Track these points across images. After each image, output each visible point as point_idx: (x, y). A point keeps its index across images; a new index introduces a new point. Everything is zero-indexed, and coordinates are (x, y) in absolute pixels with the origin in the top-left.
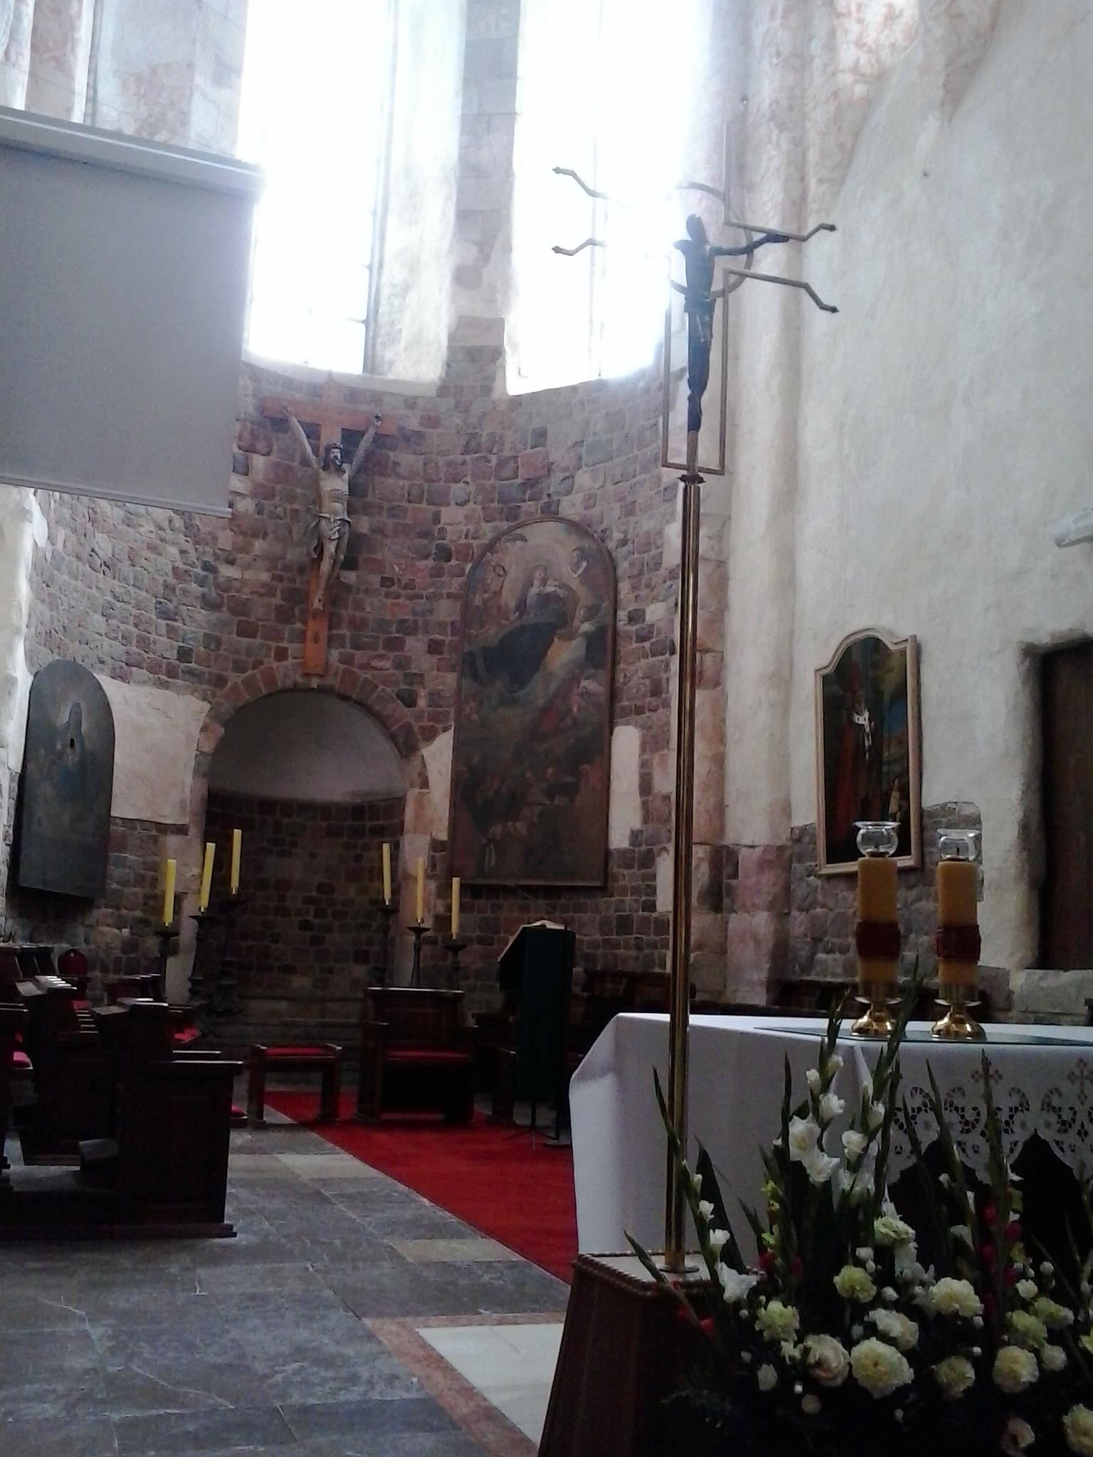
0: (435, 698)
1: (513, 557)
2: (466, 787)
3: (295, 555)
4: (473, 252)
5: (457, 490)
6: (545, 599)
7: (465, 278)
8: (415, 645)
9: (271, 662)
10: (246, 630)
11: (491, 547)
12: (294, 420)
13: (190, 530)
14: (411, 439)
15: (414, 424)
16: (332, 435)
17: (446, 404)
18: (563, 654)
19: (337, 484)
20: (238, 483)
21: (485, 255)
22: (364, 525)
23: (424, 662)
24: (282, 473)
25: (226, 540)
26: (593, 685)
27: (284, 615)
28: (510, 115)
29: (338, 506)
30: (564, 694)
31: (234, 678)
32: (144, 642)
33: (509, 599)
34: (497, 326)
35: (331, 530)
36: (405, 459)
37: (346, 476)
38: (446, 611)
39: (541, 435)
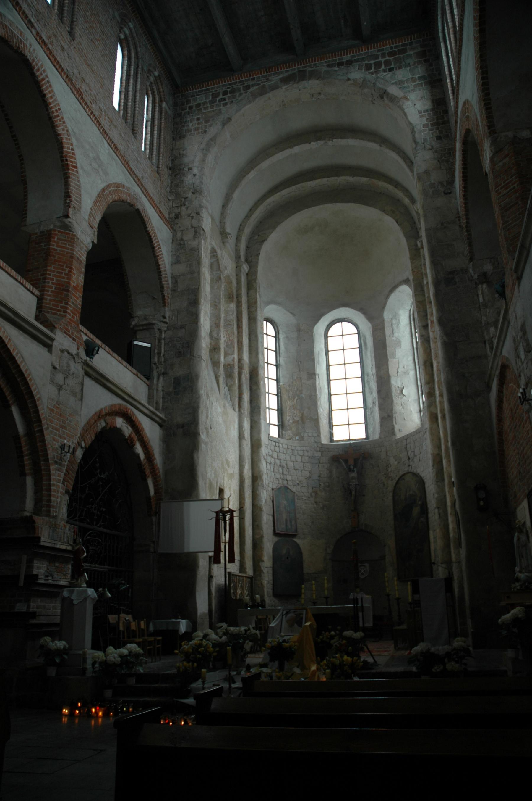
12: (341, 460)
16: (351, 462)
18: (416, 511)
29: (354, 481)
37: (356, 472)
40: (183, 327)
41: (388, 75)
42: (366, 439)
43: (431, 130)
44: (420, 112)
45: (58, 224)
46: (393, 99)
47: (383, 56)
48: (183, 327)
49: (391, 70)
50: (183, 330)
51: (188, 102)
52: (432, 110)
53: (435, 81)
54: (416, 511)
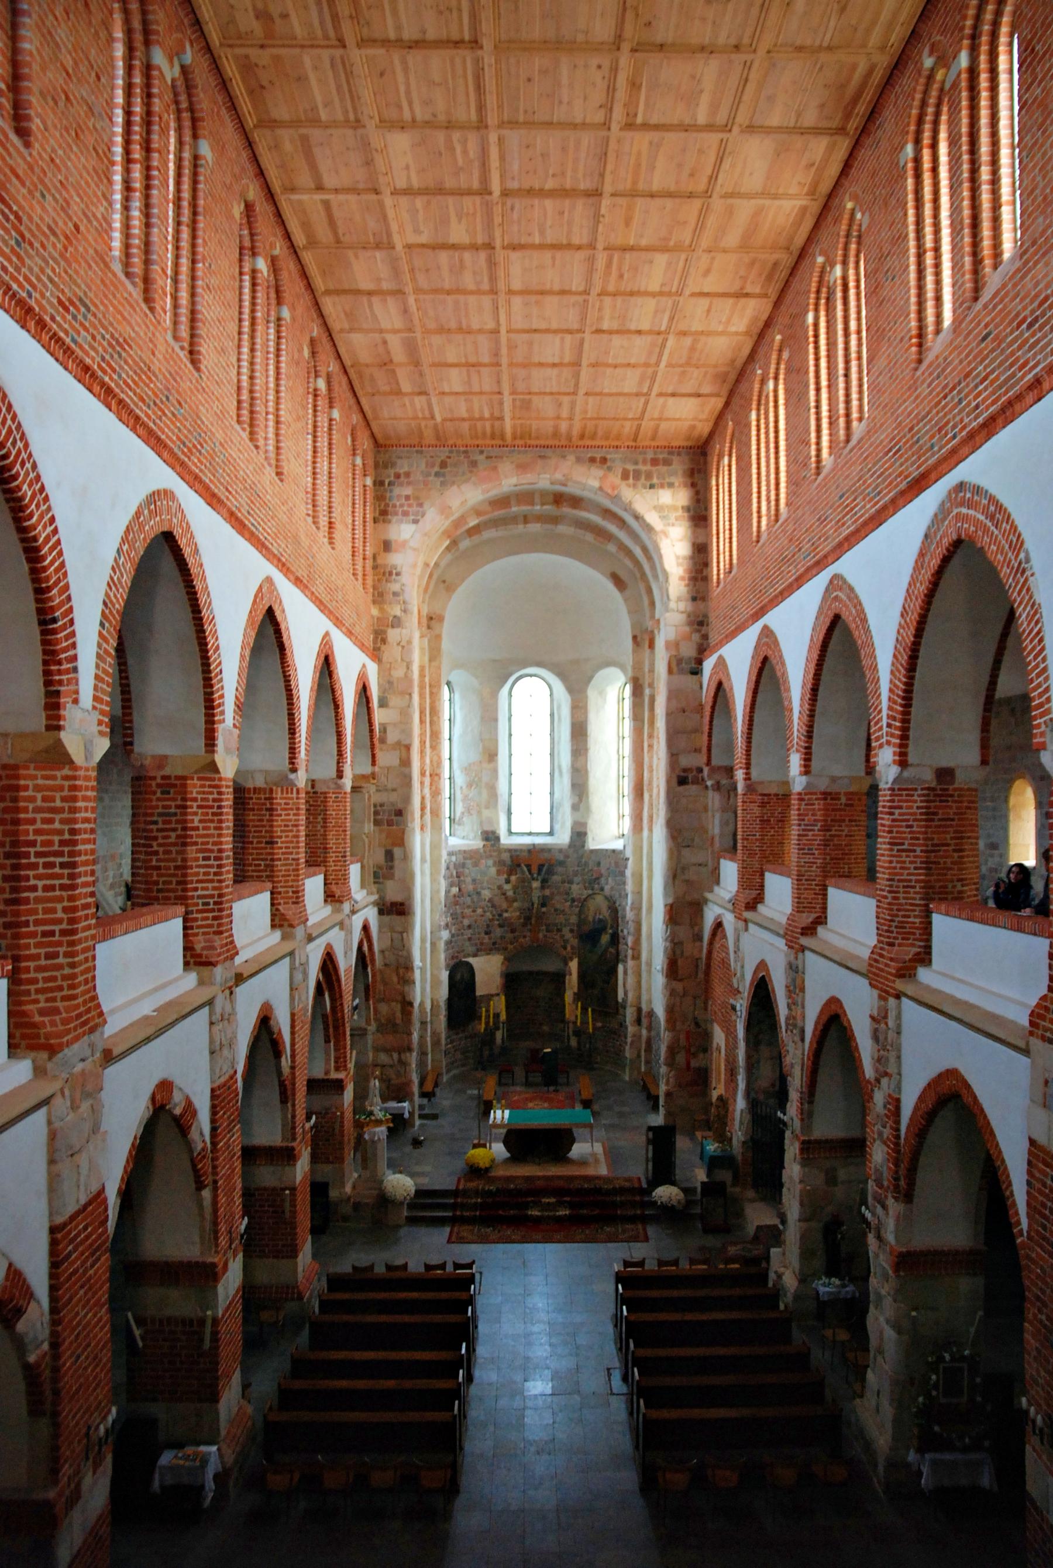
0: (573, 948)
1: (592, 905)
2: (582, 976)
3: (526, 905)
4: (577, 799)
5: (576, 879)
6: (600, 920)
7: (575, 808)
8: (566, 931)
9: (522, 940)
10: (513, 931)
11: (585, 900)
13: (493, 906)
14: (562, 863)
15: (561, 858)
16: (535, 871)
17: (571, 851)
18: (605, 939)
19: (536, 884)
20: (507, 887)
21: (581, 800)
22: (547, 892)
23: (568, 936)
24: (523, 880)
25: (505, 905)
26: (612, 950)
27: (524, 925)
28: (586, 750)
30: (606, 950)
31: (510, 947)
32: (482, 944)
33: (591, 919)
34: (584, 825)
35: (535, 900)
36: (560, 869)
38: (574, 919)
39: (599, 864)
40: (394, 790)
41: (649, 494)
42: (551, 833)
43: (688, 585)
44: (678, 557)
45: (333, 786)
46: (649, 528)
47: (644, 462)
48: (394, 790)
49: (652, 487)
50: (395, 794)
51: (393, 465)
52: (692, 558)
53: (699, 516)
54: (605, 939)
